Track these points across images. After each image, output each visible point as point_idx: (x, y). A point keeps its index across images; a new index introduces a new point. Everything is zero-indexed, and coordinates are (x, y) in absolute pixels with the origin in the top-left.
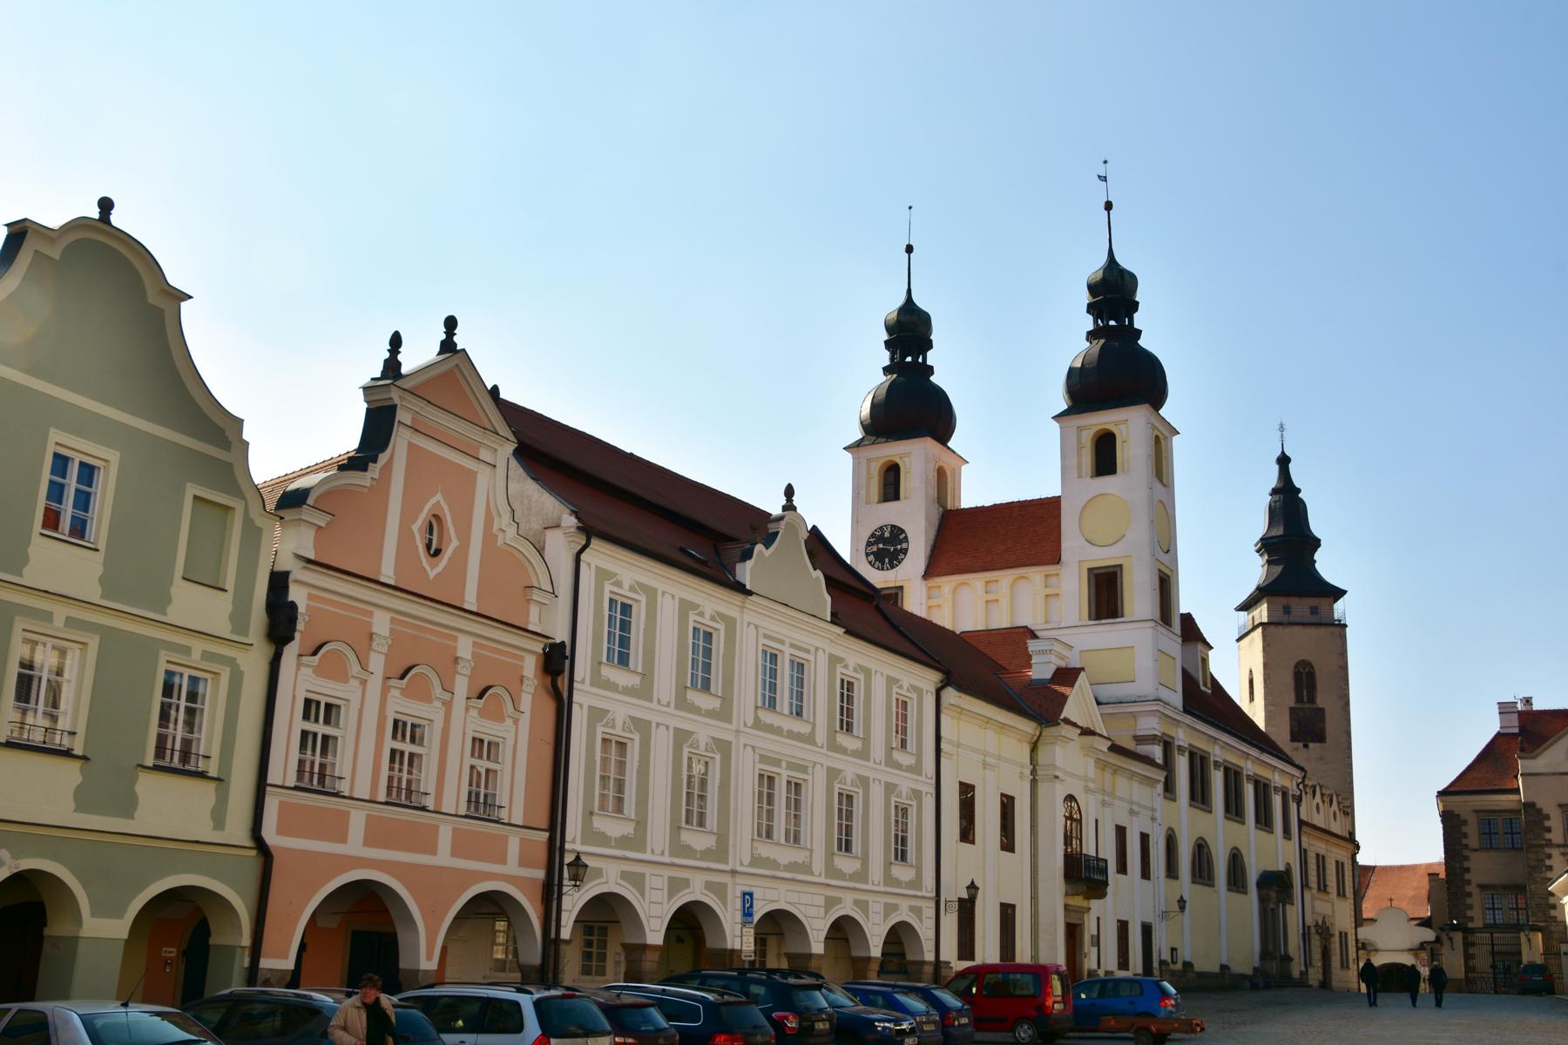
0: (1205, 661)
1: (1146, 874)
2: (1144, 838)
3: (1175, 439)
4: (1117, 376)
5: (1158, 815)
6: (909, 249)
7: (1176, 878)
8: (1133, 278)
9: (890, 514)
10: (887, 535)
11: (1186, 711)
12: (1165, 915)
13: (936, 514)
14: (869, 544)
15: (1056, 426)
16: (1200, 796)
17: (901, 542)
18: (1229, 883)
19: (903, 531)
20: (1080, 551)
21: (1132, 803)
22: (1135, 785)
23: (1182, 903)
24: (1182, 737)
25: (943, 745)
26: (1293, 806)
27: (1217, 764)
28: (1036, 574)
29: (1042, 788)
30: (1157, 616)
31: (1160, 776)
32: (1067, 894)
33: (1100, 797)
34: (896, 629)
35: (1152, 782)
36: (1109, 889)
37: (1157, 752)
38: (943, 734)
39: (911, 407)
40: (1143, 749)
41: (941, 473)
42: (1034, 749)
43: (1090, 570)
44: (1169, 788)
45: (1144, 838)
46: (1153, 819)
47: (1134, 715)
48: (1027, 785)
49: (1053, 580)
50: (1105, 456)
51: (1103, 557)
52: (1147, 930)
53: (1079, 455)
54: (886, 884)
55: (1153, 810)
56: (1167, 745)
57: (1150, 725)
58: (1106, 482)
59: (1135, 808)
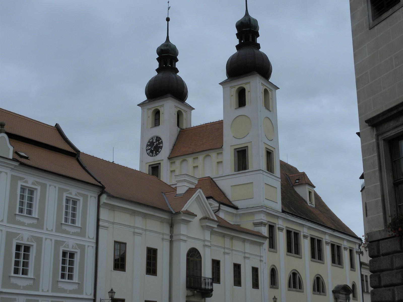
1: (256, 285)
2: (255, 271)
4: (248, 63)
6: (168, 19)
8: (256, 21)
13: (175, 130)
14: (148, 145)
18: (314, 290)
19: (160, 139)
20: (230, 141)
21: (245, 253)
22: (247, 245)
24: (280, 223)
25: (101, 223)
26: (356, 257)
28: (213, 155)
29: (175, 244)
31: (267, 242)
32: (187, 296)
34: (84, 168)
36: (213, 293)
37: (265, 231)
38: (101, 217)
39: (166, 86)
40: (257, 229)
41: (179, 114)
42: (172, 226)
43: (235, 149)
44: (272, 245)
45: (255, 271)
46: (261, 261)
48: (167, 244)
51: (240, 143)
54: (53, 291)
55: (261, 256)
56: (271, 228)
58: (242, 111)
59: (247, 255)
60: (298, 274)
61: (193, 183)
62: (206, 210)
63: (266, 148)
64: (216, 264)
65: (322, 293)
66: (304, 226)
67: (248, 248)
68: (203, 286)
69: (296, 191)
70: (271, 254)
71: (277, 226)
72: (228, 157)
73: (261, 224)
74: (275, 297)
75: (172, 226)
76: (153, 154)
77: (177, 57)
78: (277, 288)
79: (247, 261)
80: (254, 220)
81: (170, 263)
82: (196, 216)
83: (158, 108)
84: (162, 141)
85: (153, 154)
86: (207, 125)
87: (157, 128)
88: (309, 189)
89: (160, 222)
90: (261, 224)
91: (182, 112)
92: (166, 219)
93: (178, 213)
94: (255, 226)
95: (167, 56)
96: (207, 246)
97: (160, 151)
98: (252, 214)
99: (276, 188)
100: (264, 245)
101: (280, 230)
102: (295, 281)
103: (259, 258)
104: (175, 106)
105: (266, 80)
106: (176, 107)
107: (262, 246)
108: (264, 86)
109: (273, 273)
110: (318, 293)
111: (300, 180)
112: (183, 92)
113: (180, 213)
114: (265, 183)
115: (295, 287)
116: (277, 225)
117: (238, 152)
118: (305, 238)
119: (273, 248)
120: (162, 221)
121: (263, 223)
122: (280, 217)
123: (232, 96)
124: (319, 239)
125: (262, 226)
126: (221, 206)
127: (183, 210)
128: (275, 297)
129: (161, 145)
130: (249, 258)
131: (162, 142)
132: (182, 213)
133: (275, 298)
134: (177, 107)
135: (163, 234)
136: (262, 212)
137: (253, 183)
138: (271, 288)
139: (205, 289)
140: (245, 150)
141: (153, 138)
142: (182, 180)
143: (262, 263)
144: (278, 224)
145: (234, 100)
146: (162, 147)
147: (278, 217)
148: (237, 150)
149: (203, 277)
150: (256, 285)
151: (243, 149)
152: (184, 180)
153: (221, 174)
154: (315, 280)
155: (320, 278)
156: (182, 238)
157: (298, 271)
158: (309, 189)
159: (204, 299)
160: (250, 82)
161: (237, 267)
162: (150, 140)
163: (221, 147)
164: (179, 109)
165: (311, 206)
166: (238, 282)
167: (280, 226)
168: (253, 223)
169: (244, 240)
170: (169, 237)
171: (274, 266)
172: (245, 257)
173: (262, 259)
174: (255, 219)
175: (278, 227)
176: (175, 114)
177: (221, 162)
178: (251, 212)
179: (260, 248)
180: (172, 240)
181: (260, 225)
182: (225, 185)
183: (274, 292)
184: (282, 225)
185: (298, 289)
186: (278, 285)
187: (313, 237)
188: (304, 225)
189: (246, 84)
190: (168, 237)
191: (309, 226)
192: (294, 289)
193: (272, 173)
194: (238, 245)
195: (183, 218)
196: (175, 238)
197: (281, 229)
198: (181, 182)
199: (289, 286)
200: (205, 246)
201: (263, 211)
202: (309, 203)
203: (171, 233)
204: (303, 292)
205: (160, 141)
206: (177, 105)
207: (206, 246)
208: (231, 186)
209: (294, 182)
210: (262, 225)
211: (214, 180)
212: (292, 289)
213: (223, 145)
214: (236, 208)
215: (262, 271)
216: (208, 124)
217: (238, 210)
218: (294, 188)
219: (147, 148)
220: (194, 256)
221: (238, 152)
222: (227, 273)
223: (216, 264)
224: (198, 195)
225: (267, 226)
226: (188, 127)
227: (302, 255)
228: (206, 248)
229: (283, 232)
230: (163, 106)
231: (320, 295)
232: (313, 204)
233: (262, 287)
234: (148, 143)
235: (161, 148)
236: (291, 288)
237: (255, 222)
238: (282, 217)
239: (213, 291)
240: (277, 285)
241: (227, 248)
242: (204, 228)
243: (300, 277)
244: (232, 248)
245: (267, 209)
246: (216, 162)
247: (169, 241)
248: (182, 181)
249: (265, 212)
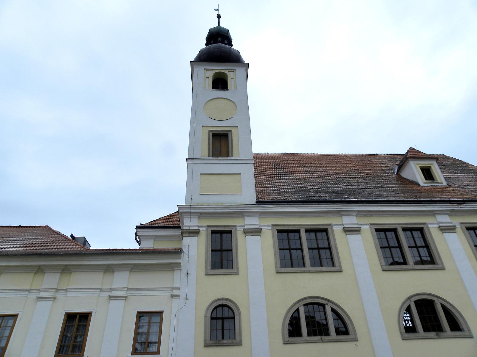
60: (329, 304)
66: (341, 213)
78: (239, 344)
101: (247, 234)
118: (347, 233)
143: (175, 301)
147: (241, 215)
155: (434, 301)
173: (175, 292)
188: (339, 212)
191: (359, 211)
204: (355, 340)
232: (439, 181)
238: (257, 212)
241: (46, 290)
249: (191, 213)
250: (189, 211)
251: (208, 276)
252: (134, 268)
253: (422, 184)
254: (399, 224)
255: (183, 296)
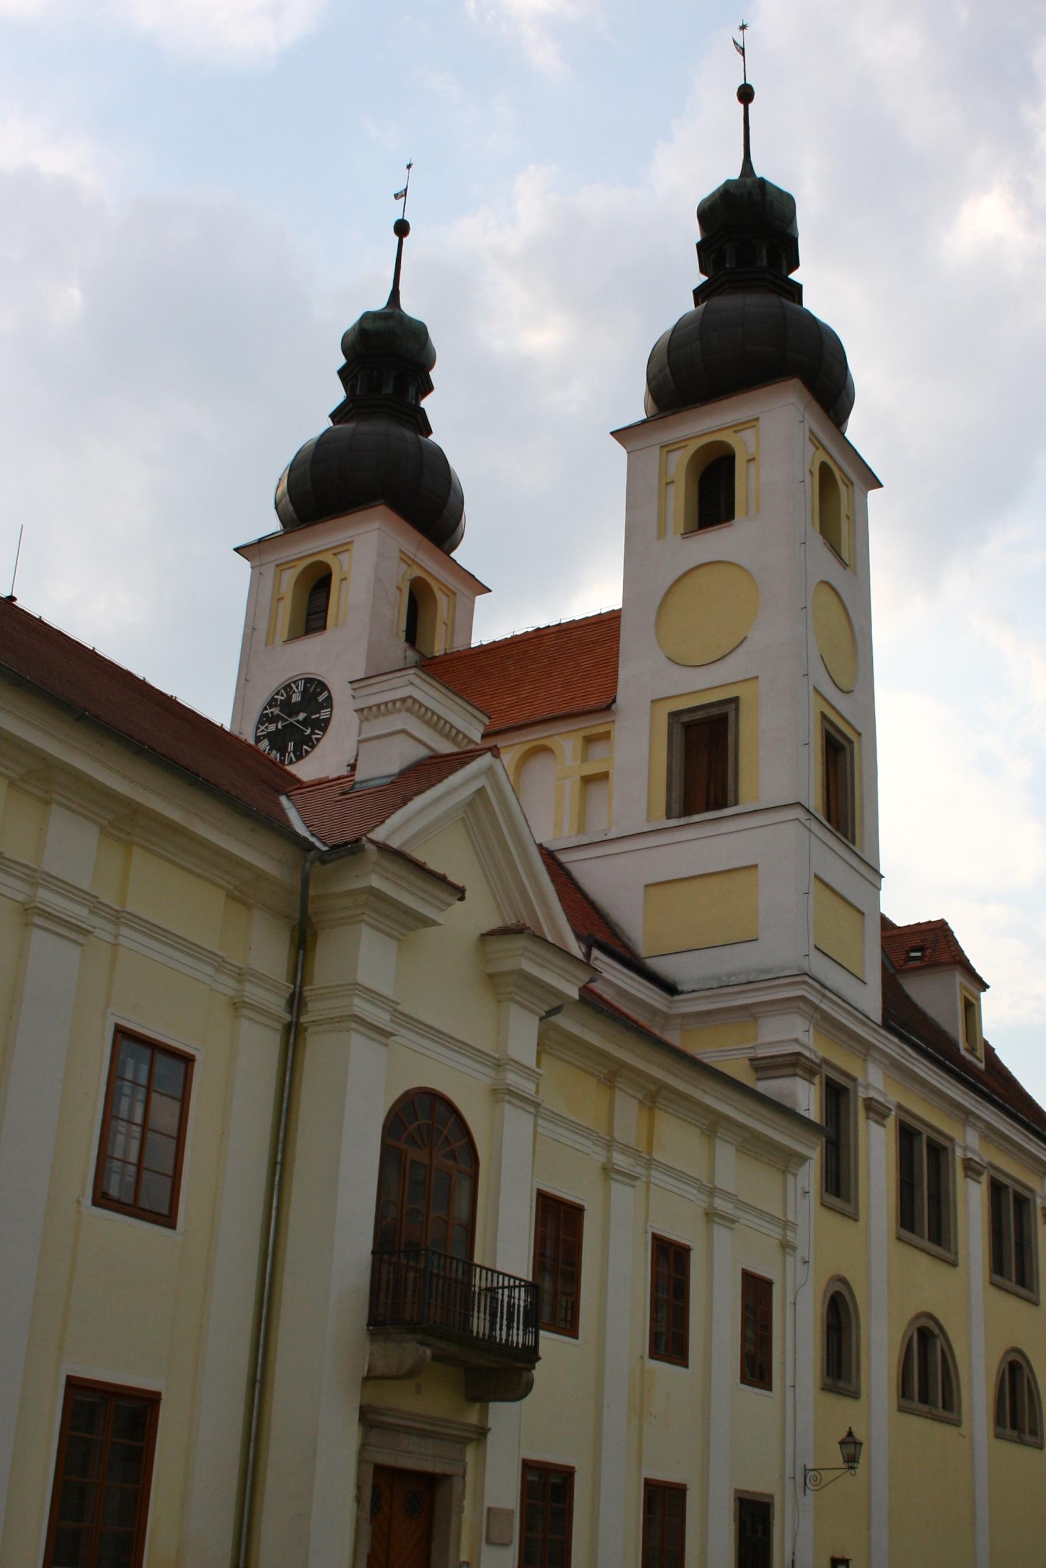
0: (971, 1010)
1: (757, 1369)
2: (757, 1293)
3: (873, 495)
5: (801, 1238)
7: (854, 1394)
9: (310, 657)
10: (296, 698)
11: (886, 1025)
12: (810, 1478)
15: (619, 454)
16: (924, 1216)
17: (321, 707)
19: (323, 686)
20: (650, 685)
21: (712, 1192)
22: (726, 1153)
23: (851, 1448)
24: (874, 1081)
27: (971, 1168)
28: (566, 743)
29: (317, 1049)
30: (815, 799)
32: (370, 1378)
33: (599, 1156)
35: (787, 1161)
36: (539, 1372)
40: (767, 1087)
42: (303, 940)
43: (673, 716)
44: (838, 1183)
45: (757, 1293)
46: (786, 1247)
47: (749, 1013)
49: (599, 750)
50: (715, 492)
51: (698, 686)
52: (754, 1517)
53: (662, 498)
55: (786, 1225)
56: (836, 1095)
57: (788, 1033)
59: (722, 1205)
61: (449, 732)
62: (523, 891)
63: (824, 717)
64: (559, 1224)
65: (1027, 1437)
66: (972, 1120)
67: (729, 1167)
68: (479, 1324)
69: (907, 998)
70: (832, 1222)
71: (860, 1094)
72: (638, 750)
73: (795, 1065)
74: (850, 1434)
75: (303, 940)
76: (283, 755)
77: (431, 373)
79: (720, 1233)
80: (753, 1048)
81: (274, 1164)
82: (462, 899)
83: (327, 558)
84: (329, 699)
85: (283, 755)
86: (542, 633)
87: (313, 644)
88: (965, 989)
89: (229, 895)
90: (794, 1064)
91: (434, 595)
92: (261, 876)
93: (349, 849)
94: (761, 1074)
95: (388, 360)
96: (511, 1093)
97: (318, 740)
98: (749, 1013)
99: (863, 914)
100: (803, 1171)
101: (871, 1115)
102: (927, 1372)
103: (776, 1232)
104: (401, 551)
105: (831, 425)
106: (406, 559)
107: (795, 1175)
108: (821, 452)
109: (839, 1315)
110: (1015, 1434)
111: (929, 951)
112: (446, 502)
113: (362, 849)
114: (817, 877)
115: (924, 1398)
116: (860, 1089)
117: (687, 727)
118: (969, 1173)
119: (838, 1194)
120: (243, 891)
121: (803, 1060)
122: (874, 1054)
123: (668, 483)
124: (1020, 1189)
125: (795, 1075)
126: (596, 959)
127: (379, 834)
128: (850, 1434)
129: (324, 714)
130: (733, 1221)
131: (329, 702)
132: (370, 847)
133: (850, 1439)
134: (410, 563)
135: (241, 975)
136: (801, 1005)
137: (755, 866)
138: (825, 1388)
139: (489, 1345)
140: (723, 719)
141: (289, 686)
142: (394, 702)
144: (867, 1086)
145: (679, 501)
146: (327, 721)
147: (865, 1050)
148: (685, 719)
149: (482, 1268)
150: (757, 1369)
151: (715, 711)
152: (403, 700)
153: (599, 826)
154: (1003, 1374)
155: (1020, 1367)
156: (362, 1007)
157: (942, 1321)
158: (965, 989)
159: (478, 1405)
160: (757, 419)
161: (670, 1261)
162: (277, 694)
163: (607, 707)
164: (417, 573)
165: (970, 1062)
166: (669, 1340)
167: (872, 1094)
168: (751, 1060)
169: (714, 1125)
170: (283, 1003)
171: (842, 1280)
172: (711, 1216)
174: (760, 1041)
175: (865, 1096)
176: (398, 588)
177: (604, 776)
178: (745, 1007)
179: (785, 1183)
180: (298, 1024)
181: (790, 1071)
182: (616, 883)
183: (843, 1414)
184: (885, 1095)
185: (940, 1411)
186: (858, 1379)
187: (1002, 1179)
188: (968, 1113)
189: (737, 428)
190: (276, 1003)
191: (989, 1126)
192: (925, 1408)
193: (847, 837)
194: (678, 1141)
195: (376, 882)
196: (315, 1010)
197: (876, 1110)
198: (388, 712)
199: (904, 1391)
200: (501, 1093)
201: (802, 998)
202: (966, 1050)
203: (294, 983)
205: (321, 699)
206: (410, 549)
207: (507, 1098)
208: (647, 886)
209: (903, 957)
210: (799, 1071)
211: (563, 858)
212: (917, 1405)
213: (614, 701)
214: (670, 988)
215: (790, 1299)
216: (548, 631)
217: (677, 998)
218: (901, 981)
219: (258, 728)
220: (427, 1142)
221: (687, 727)
222: (615, 1284)
223: (559, 1224)
224: (481, 792)
225: (817, 1079)
226: (458, 646)
227: (956, 1253)
228: (507, 1108)
229: (884, 1126)
230: (348, 550)
231: (1022, 1442)
232: (978, 1054)
233: (789, 1382)
234: (265, 709)
235: (324, 725)
236: (912, 1399)
237: (761, 1053)
239: (538, 1365)
240: (854, 1381)
242: (500, 985)
243: (948, 1353)
244: (650, 1153)
245: (824, 995)
246: (578, 778)
247: (279, 1026)
248: (390, 705)
249: (816, 1008)
250: (817, 1002)
251: (822, 1209)
252: (753, 1145)
253: (963, 1052)
254: (1013, 1179)
255: (801, 1252)
